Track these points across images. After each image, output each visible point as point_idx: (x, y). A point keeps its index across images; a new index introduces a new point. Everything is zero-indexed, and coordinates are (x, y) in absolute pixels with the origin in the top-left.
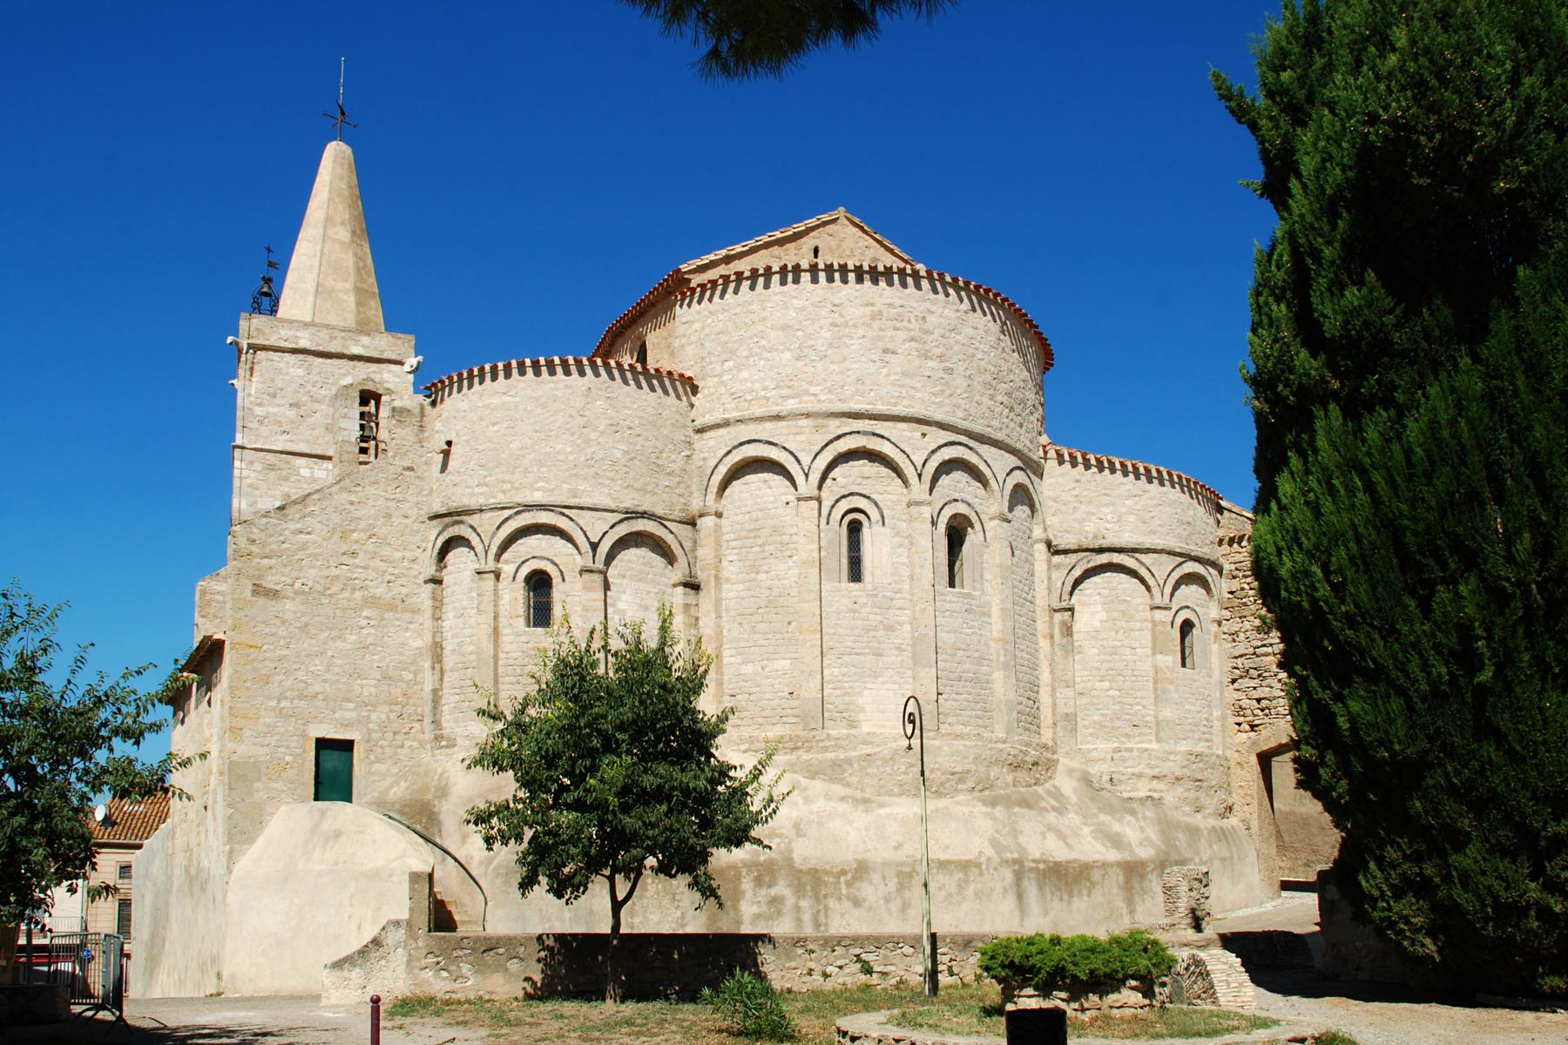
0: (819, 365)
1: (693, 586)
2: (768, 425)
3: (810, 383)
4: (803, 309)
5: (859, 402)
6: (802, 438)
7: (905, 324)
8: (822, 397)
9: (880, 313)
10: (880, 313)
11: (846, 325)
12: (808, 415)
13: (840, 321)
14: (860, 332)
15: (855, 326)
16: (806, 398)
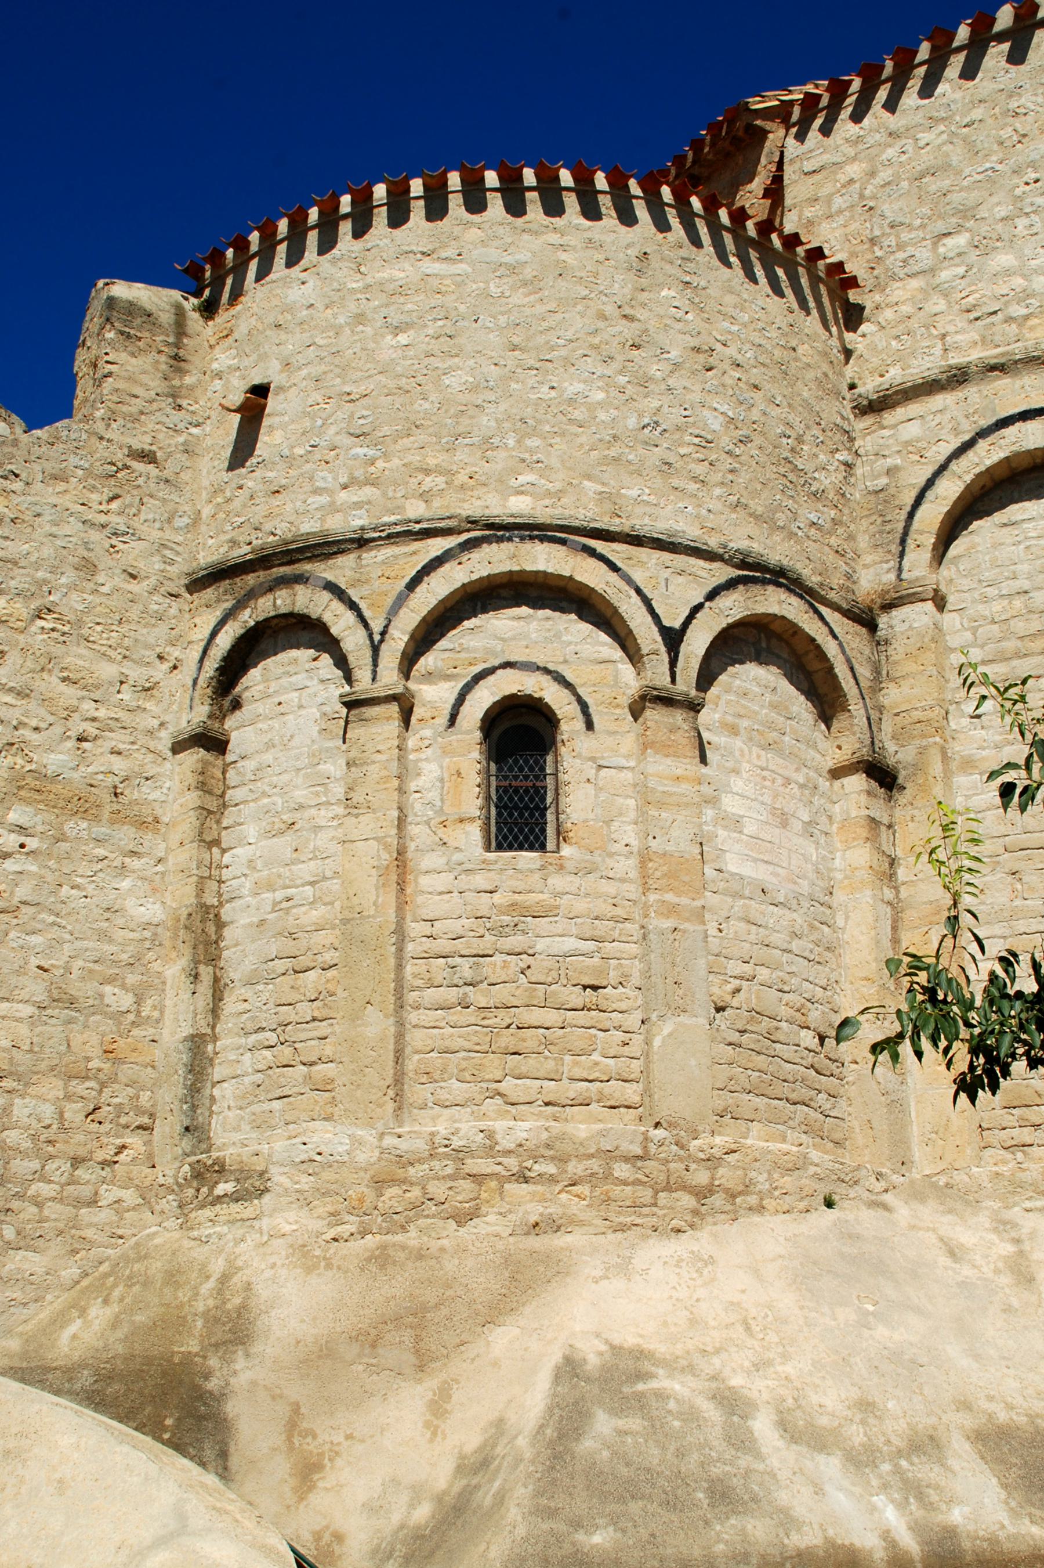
1: (883, 776)
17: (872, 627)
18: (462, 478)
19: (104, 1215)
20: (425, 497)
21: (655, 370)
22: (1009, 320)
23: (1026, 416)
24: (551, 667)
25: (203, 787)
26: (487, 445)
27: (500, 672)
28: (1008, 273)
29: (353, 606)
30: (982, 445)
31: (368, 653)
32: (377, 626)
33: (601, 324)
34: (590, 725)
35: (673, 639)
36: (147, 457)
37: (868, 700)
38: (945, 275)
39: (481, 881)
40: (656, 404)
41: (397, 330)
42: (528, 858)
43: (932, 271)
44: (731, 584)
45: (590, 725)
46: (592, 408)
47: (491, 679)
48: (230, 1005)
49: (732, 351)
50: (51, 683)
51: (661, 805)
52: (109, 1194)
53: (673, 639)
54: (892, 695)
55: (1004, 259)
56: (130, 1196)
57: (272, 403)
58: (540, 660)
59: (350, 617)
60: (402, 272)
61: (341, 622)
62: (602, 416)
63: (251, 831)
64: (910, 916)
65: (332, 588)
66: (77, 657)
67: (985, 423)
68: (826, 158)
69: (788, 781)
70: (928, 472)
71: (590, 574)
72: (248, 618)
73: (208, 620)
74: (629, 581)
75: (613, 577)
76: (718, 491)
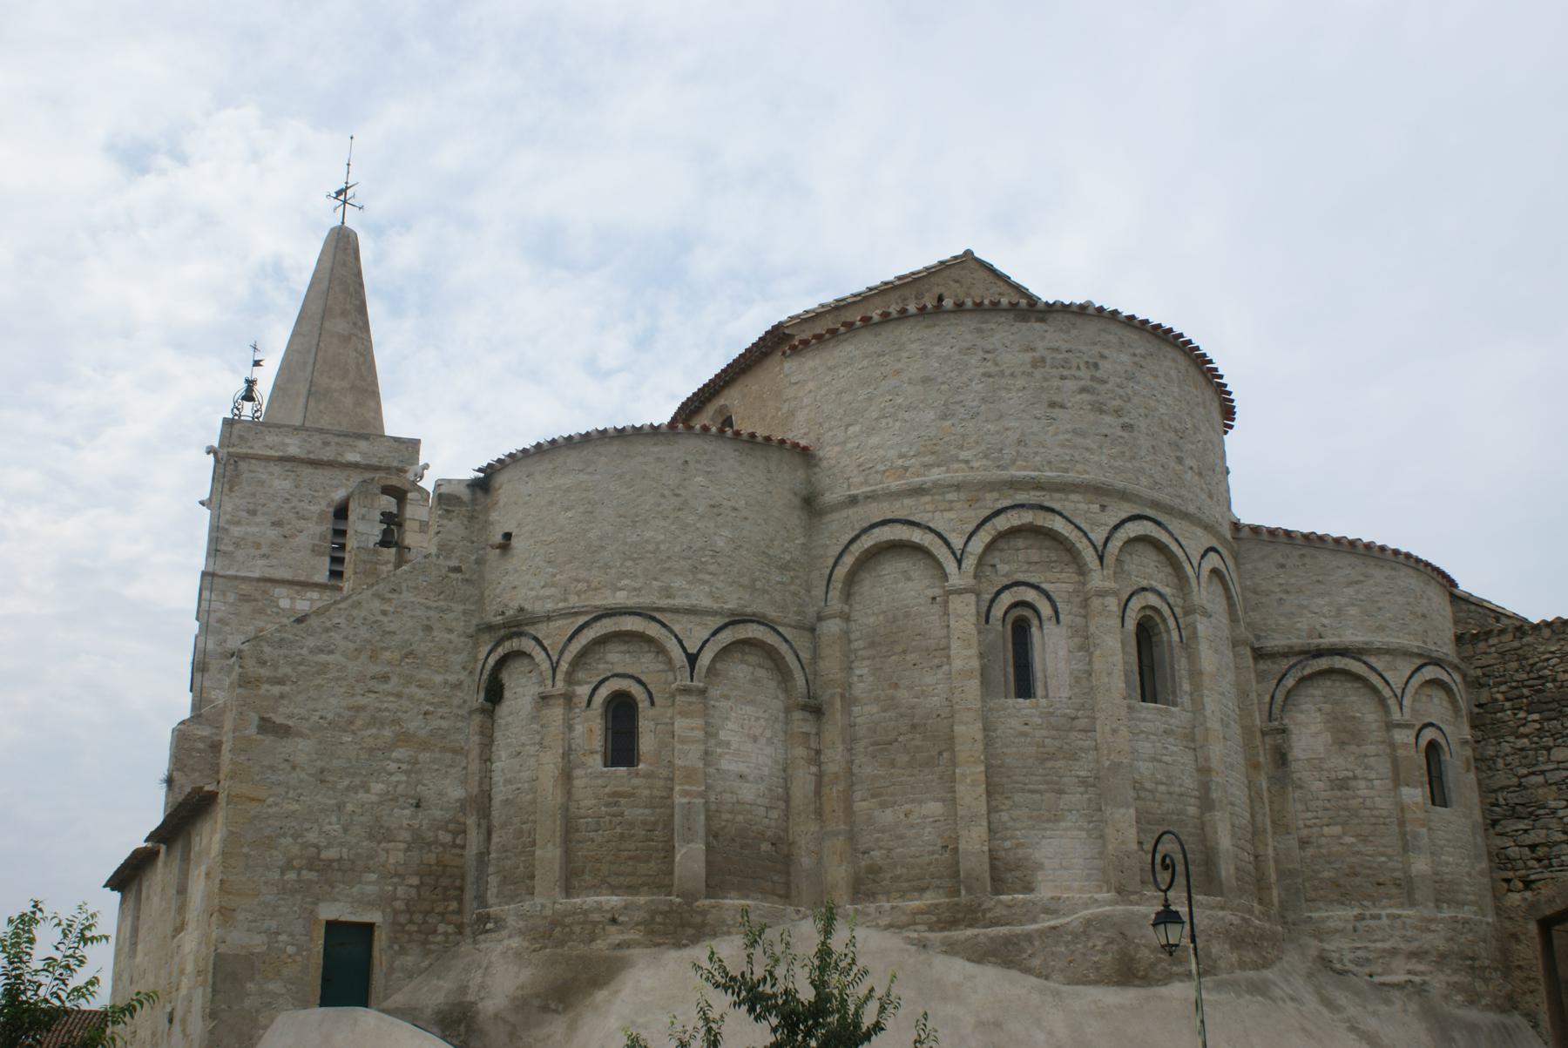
0: (971, 425)
2: (907, 501)
3: (961, 448)
4: (949, 357)
6: (952, 515)
7: (1073, 372)
8: (975, 464)
9: (1043, 360)
10: (1043, 360)
11: (1002, 374)
12: (958, 487)
13: (992, 368)
14: (1020, 383)
15: (1012, 375)
16: (956, 466)
17: (813, 630)
18: (594, 585)
19: (440, 938)
20: (578, 594)
21: (691, 519)
23: (884, 523)
25: (482, 733)
26: (606, 567)
28: (878, 447)
29: (545, 649)
30: (864, 538)
31: (550, 672)
32: (555, 659)
34: (653, 703)
35: (692, 659)
36: (458, 570)
38: (849, 446)
39: (600, 782)
41: (567, 509)
42: (622, 770)
43: (845, 443)
44: (725, 626)
45: (653, 703)
46: (658, 544)
48: (495, 839)
49: (732, 503)
50: (413, 689)
51: (683, 742)
52: (441, 928)
53: (692, 659)
54: (823, 665)
55: (875, 440)
56: (451, 929)
57: (514, 542)
58: (630, 671)
59: (543, 654)
60: (568, 481)
61: (539, 655)
62: (662, 547)
63: (503, 755)
64: (826, 779)
65: (536, 639)
66: (423, 674)
67: (865, 525)
68: (800, 377)
69: (757, 719)
70: (840, 549)
71: (653, 630)
72: (501, 651)
73: (485, 649)
74: (671, 631)
75: (663, 631)
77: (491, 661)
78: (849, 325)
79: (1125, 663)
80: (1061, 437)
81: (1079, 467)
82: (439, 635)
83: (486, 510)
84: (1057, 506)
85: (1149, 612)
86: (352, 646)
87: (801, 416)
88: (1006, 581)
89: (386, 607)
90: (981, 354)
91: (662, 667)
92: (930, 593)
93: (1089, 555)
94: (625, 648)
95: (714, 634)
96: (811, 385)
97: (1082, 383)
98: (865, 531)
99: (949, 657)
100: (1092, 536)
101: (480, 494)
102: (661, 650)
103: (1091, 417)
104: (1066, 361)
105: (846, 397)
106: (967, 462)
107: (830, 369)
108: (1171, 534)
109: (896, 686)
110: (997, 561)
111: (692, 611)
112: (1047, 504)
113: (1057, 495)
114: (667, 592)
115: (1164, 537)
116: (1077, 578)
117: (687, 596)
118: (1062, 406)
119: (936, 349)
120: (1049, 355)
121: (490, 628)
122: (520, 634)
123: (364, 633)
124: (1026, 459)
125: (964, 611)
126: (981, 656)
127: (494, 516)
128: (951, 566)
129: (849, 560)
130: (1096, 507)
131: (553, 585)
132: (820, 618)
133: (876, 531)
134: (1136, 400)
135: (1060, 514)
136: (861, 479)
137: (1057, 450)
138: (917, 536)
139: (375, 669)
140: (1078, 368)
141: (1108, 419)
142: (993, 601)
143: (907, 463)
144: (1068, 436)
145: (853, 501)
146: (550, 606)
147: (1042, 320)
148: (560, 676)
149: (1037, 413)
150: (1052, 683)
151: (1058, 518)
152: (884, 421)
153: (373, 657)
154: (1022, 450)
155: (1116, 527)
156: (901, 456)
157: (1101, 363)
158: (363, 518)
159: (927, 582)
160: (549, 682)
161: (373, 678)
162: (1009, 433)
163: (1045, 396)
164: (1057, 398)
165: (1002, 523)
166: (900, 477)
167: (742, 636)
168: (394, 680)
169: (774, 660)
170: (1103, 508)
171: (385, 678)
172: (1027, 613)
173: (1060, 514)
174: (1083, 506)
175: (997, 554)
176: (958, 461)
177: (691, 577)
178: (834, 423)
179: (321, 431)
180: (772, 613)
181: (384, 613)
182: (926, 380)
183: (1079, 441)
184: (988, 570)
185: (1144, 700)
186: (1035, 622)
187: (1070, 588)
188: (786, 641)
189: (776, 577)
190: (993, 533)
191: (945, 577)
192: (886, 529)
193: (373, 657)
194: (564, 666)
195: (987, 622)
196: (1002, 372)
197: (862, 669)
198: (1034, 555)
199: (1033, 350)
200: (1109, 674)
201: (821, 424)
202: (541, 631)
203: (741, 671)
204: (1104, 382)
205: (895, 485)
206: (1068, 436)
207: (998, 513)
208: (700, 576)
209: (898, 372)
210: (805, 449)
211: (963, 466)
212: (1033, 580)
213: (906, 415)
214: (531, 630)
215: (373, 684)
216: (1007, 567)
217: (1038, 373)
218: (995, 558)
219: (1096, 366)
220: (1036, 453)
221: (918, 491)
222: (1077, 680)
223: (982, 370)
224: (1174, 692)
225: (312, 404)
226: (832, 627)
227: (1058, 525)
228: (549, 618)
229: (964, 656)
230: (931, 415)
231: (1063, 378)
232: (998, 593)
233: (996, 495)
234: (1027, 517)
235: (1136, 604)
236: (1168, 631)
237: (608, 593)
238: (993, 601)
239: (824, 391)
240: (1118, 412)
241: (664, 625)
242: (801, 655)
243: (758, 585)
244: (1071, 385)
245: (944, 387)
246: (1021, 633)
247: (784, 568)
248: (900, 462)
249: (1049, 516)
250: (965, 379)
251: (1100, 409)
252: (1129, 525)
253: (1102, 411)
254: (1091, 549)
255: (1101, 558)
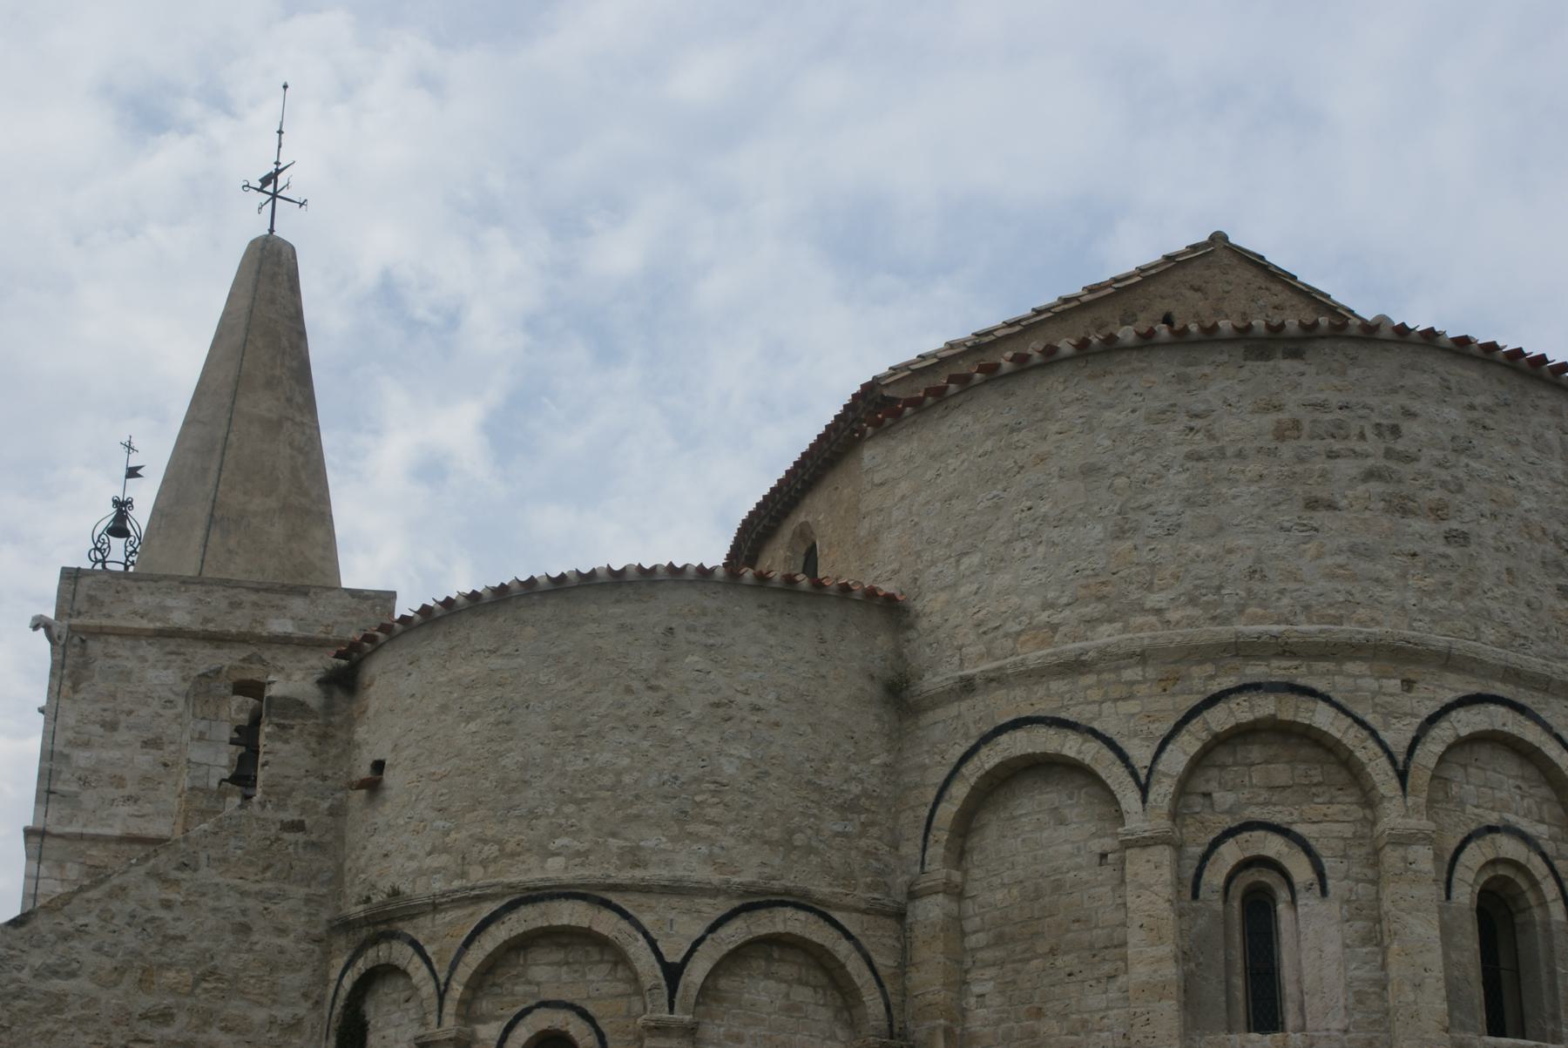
0: (1165, 546)
2: (1057, 686)
3: (1149, 587)
5: (1256, 620)
6: (1132, 706)
8: (1173, 616)
9: (1296, 425)
10: (1296, 425)
12: (1142, 657)
13: (1205, 446)
14: (1254, 468)
15: (1240, 455)
16: (1139, 620)
17: (900, 915)
18: (510, 847)
20: (484, 864)
21: (677, 729)
22: (1006, 635)
24: (578, 1003)
26: (532, 815)
27: (536, 1011)
29: (427, 961)
30: (984, 751)
31: (435, 1001)
32: (442, 977)
33: (628, 698)
36: (297, 826)
37: (888, 987)
40: (676, 760)
41: (469, 719)
43: (954, 586)
46: (619, 774)
47: (529, 1018)
49: (753, 698)
54: (916, 977)
55: (1005, 579)
57: (389, 777)
58: (567, 996)
59: (424, 970)
61: (419, 972)
62: (627, 779)
66: (234, 1008)
70: (946, 771)
71: (606, 924)
72: (361, 965)
73: (339, 962)
76: (731, 828)
77: (347, 983)
78: (964, 380)
79: (1448, 963)
80: (1329, 561)
81: (1362, 613)
82: (262, 939)
83: (350, 723)
84: (1320, 685)
85: (1502, 871)
86: (108, 964)
87: (889, 541)
88: (1229, 822)
89: (172, 896)
90: (1184, 420)
91: (621, 987)
92: (1097, 846)
93: (1380, 773)
94: (559, 955)
95: (713, 928)
96: (904, 487)
97: (1370, 462)
98: (986, 739)
99: (1125, 959)
100: (1386, 736)
101: (339, 695)
102: (620, 959)
103: (1385, 522)
104: (1340, 425)
105: (959, 506)
106: (1158, 612)
107: (933, 457)
108: (1547, 728)
109: (1039, 1013)
110: (1213, 786)
111: (675, 889)
112: (1301, 681)
113: (1321, 666)
114: (634, 857)
115: (1531, 733)
116: (1359, 813)
117: (668, 863)
118: (1331, 506)
119: (1108, 414)
120: (1306, 418)
121: (346, 925)
122: (391, 936)
123: (130, 939)
124: (1263, 604)
125: (1153, 874)
126: (1183, 956)
127: (361, 733)
128: (1129, 797)
129: (960, 791)
130: (1393, 684)
131: (446, 850)
132: (913, 895)
133: (1004, 739)
134: (1473, 488)
135: (1327, 699)
136: (981, 648)
137: (1323, 585)
138: (1072, 746)
139: (145, 1002)
140: (1362, 436)
141: (1417, 525)
142: (1205, 857)
143: (1056, 619)
144: (1341, 559)
145: (967, 687)
146: (438, 886)
147: (1296, 355)
148: (450, 1007)
149: (1286, 520)
150: (1313, 1005)
151: (1321, 705)
152: (1019, 545)
153: (144, 983)
154: (1257, 586)
155: (1432, 720)
156: (1048, 605)
157: (1407, 427)
158: (201, 737)
159: (1091, 827)
160: (433, 1018)
161: (143, 1017)
162: (1234, 558)
163: (1298, 489)
164: (1321, 493)
165: (1220, 719)
166: (1044, 643)
167: (763, 931)
168: (182, 1019)
169: (827, 971)
170: (1408, 685)
171: (166, 1017)
172: (1269, 878)
173: (1327, 699)
174: (1370, 683)
175: (1213, 773)
176: (1144, 611)
177: (676, 830)
178: (939, 552)
179: (226, 583)
180: (821, 888)
181: (167, 905)
182: (1089, 471)
183: (1363, 565)
184: (1197, 803)
185: (1496, 1027)
186: (1283, 895)
187: (1348, 830)
188: (848, 936)
189: (832, 823)
190: (1204, 735)
191: (1119, 817)
192: (1020, 734)
193: (144, 983)
194: (457, 990)
195: (1195, 896)
196: (1222, 450)
197: (983, 984)
198: (1281, 773)
199: (1279, 408)
200: (1418, 986)
201: (918, 555)
202: (421, 929)
203: (762, 991)
204: (1408, 458)
205: (1034, 656)
206: (1341, 559)
207: (1212, 701)
208: (691, 828)
209: (1042, 459)
210: (890, 598)
211: (1153, 619)
212: (1277, 819)
213: (1055, 534)
214: (406, 928)
215: (143, 1027)
216: (1228, 797)
217: (1287, 450)
218: (1209, 781)
219: (1395, 431)
220: (1282, 592)
221: (1075, 667)
222: (1360, 998)
223: (1186, 449)
224: (1555, 1017)
225: (215, 538)
226: (932, 910)
227: (1322, 718)
228: (435, 907)
229: (1152, 959)
230: (1098, 531)
231: (1332, 455)
232: (1215, 844)
233: (1209, 668)
234: (1266, 707)
235: (1475, 856)
236: (1543, 904)
237: (533, 861)
238: (1205, 857)
239: (921, 499)
240: (1438, 512)
241: (625, 915)
242: (878, 960)
243: (799, 839)
244: (1346, 468)
245: (1121, 482)
246: (1258, 913)
247: (848, 808)
248: (1044, 616)
249: (1306, 703)
250: (1155, 467)
251: (1401, 507)
252: (1460, 715)
253: (1405, 512)
254: (1383, 762)
255: (1402, 776)
